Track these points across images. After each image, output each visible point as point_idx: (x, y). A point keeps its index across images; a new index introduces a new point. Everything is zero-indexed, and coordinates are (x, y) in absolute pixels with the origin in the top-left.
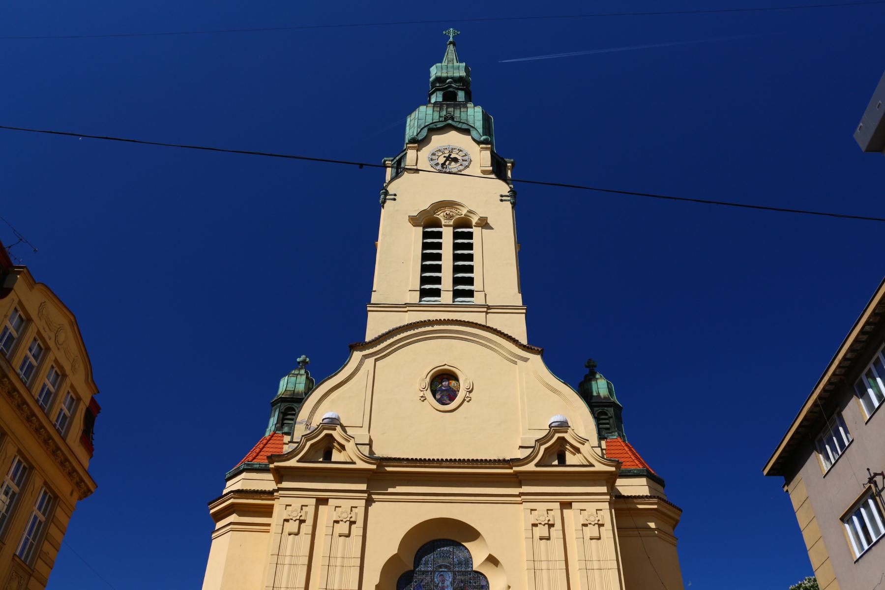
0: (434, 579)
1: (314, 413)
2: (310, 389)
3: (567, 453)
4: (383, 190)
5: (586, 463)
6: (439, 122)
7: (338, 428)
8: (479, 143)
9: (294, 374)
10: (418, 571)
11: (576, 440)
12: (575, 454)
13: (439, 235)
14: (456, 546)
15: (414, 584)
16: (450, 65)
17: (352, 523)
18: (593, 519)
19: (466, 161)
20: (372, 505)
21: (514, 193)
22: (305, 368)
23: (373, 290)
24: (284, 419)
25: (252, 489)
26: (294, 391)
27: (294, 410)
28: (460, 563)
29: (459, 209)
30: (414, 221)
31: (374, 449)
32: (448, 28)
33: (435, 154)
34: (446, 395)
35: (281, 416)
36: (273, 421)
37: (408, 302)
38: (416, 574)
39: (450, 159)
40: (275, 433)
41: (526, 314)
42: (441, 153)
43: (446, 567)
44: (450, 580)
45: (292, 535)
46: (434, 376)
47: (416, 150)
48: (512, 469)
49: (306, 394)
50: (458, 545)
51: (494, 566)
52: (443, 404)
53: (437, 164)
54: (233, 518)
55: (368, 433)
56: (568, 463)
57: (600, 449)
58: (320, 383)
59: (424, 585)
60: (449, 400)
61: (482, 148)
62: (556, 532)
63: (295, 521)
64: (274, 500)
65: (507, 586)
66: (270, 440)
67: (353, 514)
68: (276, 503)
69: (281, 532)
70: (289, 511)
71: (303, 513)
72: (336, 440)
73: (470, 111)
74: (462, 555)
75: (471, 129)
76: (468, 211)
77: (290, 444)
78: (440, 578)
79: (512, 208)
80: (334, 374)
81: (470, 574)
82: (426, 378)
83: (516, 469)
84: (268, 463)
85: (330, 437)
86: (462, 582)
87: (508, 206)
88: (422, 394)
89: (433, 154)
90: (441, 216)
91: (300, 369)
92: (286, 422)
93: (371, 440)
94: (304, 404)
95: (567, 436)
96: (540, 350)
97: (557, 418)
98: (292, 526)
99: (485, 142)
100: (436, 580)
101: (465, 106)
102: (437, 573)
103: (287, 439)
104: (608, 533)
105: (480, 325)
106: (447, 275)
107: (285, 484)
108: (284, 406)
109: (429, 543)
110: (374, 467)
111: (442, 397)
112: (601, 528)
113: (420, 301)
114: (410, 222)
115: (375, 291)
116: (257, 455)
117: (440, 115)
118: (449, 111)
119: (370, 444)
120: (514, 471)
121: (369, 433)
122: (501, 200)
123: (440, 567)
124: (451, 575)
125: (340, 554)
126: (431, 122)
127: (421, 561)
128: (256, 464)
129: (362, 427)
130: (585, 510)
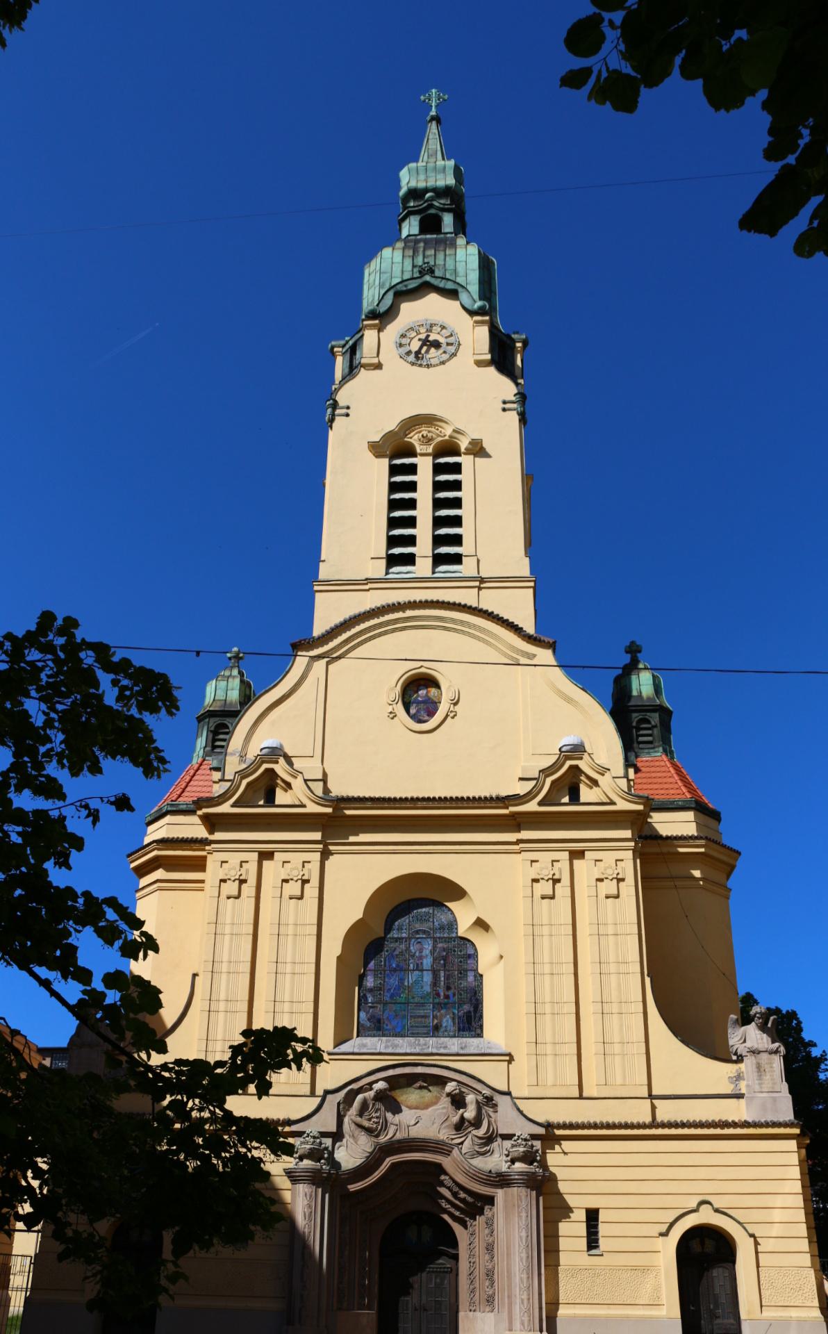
0: (409, 947)
1: (249, 741)
3: (582, 786)
4: (329, 400)
5: (605, 800)
6: (413, 278)
7: (282, 760)
8: (471, 313)
10: (390, 938)
11: (593, 769)
12: (591, 788)
13: (412, 469)
15: (384, 954)
16: (431, 165)
17: (305, 882)
19: (452, 344)
20: (329, 858)
21: (522, 397)
23: (322, 559)
28: (442, 928)
29: (441, 427)
30: (377, 449)
31: (330, 785)
32: (427, 90)
33: (406, 335)
34: (424, 709)
37: (370, 576)
38: (388, 941)
39: (428, 343)
41: (534, 588)
42: (415, 334)
43: (424, 932)
44: (430, 948)
45: (232, 899)
46: (408, 682)
47: (376, 331)
48: (508, 808)
50: (440, 905)
51: (484, 931)
52: (420, 721)
53: (409, 353)
55: (321, 765)
56: (582, 799)
57: (625, 780)
59: (397, 955)
60: (428, 715)
61: (476, 322)
62: (563, 890)
63: (234, 881)
65: (498, 956)
67: (305, 871)
70: (225, 869)
71: (243, 871)
72: (280, 777)
73: (460, 253)
74: (443, 918)
75: (460, 290)
76: (454, 431)
77: (221, 783)
78: (418, 946)
79: (520, 421)
81: (454, 941)
82: (396, 686)
83: (513, 809)
84: (195, 809)
85: (271, 773)
86: (444, 950)
87: (514, 417)
88: (390, 709)
89: (403, 336)
90: (415, 440)
93: (325, 774)
95: (582, 765)
96: (551, 642)
98: (232, 888)
99: (480, 312)
100: (412, 948)
101: (453, 245)
102: (413, 940)
103: (217, 776)
104: (629, 890)
105: (470, 607)
106: (424, 531)
107: (219, 836)
109: (402, 903)
110: (329, 810)
111: (418, 711)
112: (621, 884)
113: (387, 573)
114: (371, 451)
117: (413, 263)
118: (428, 256)
119: (324, 780)
121: (322, 764)
122: (504, 410)
124: (430, 942)
125: (291, 921)
126: (399, 280)
127: (394, 927)
130: (601, 861)
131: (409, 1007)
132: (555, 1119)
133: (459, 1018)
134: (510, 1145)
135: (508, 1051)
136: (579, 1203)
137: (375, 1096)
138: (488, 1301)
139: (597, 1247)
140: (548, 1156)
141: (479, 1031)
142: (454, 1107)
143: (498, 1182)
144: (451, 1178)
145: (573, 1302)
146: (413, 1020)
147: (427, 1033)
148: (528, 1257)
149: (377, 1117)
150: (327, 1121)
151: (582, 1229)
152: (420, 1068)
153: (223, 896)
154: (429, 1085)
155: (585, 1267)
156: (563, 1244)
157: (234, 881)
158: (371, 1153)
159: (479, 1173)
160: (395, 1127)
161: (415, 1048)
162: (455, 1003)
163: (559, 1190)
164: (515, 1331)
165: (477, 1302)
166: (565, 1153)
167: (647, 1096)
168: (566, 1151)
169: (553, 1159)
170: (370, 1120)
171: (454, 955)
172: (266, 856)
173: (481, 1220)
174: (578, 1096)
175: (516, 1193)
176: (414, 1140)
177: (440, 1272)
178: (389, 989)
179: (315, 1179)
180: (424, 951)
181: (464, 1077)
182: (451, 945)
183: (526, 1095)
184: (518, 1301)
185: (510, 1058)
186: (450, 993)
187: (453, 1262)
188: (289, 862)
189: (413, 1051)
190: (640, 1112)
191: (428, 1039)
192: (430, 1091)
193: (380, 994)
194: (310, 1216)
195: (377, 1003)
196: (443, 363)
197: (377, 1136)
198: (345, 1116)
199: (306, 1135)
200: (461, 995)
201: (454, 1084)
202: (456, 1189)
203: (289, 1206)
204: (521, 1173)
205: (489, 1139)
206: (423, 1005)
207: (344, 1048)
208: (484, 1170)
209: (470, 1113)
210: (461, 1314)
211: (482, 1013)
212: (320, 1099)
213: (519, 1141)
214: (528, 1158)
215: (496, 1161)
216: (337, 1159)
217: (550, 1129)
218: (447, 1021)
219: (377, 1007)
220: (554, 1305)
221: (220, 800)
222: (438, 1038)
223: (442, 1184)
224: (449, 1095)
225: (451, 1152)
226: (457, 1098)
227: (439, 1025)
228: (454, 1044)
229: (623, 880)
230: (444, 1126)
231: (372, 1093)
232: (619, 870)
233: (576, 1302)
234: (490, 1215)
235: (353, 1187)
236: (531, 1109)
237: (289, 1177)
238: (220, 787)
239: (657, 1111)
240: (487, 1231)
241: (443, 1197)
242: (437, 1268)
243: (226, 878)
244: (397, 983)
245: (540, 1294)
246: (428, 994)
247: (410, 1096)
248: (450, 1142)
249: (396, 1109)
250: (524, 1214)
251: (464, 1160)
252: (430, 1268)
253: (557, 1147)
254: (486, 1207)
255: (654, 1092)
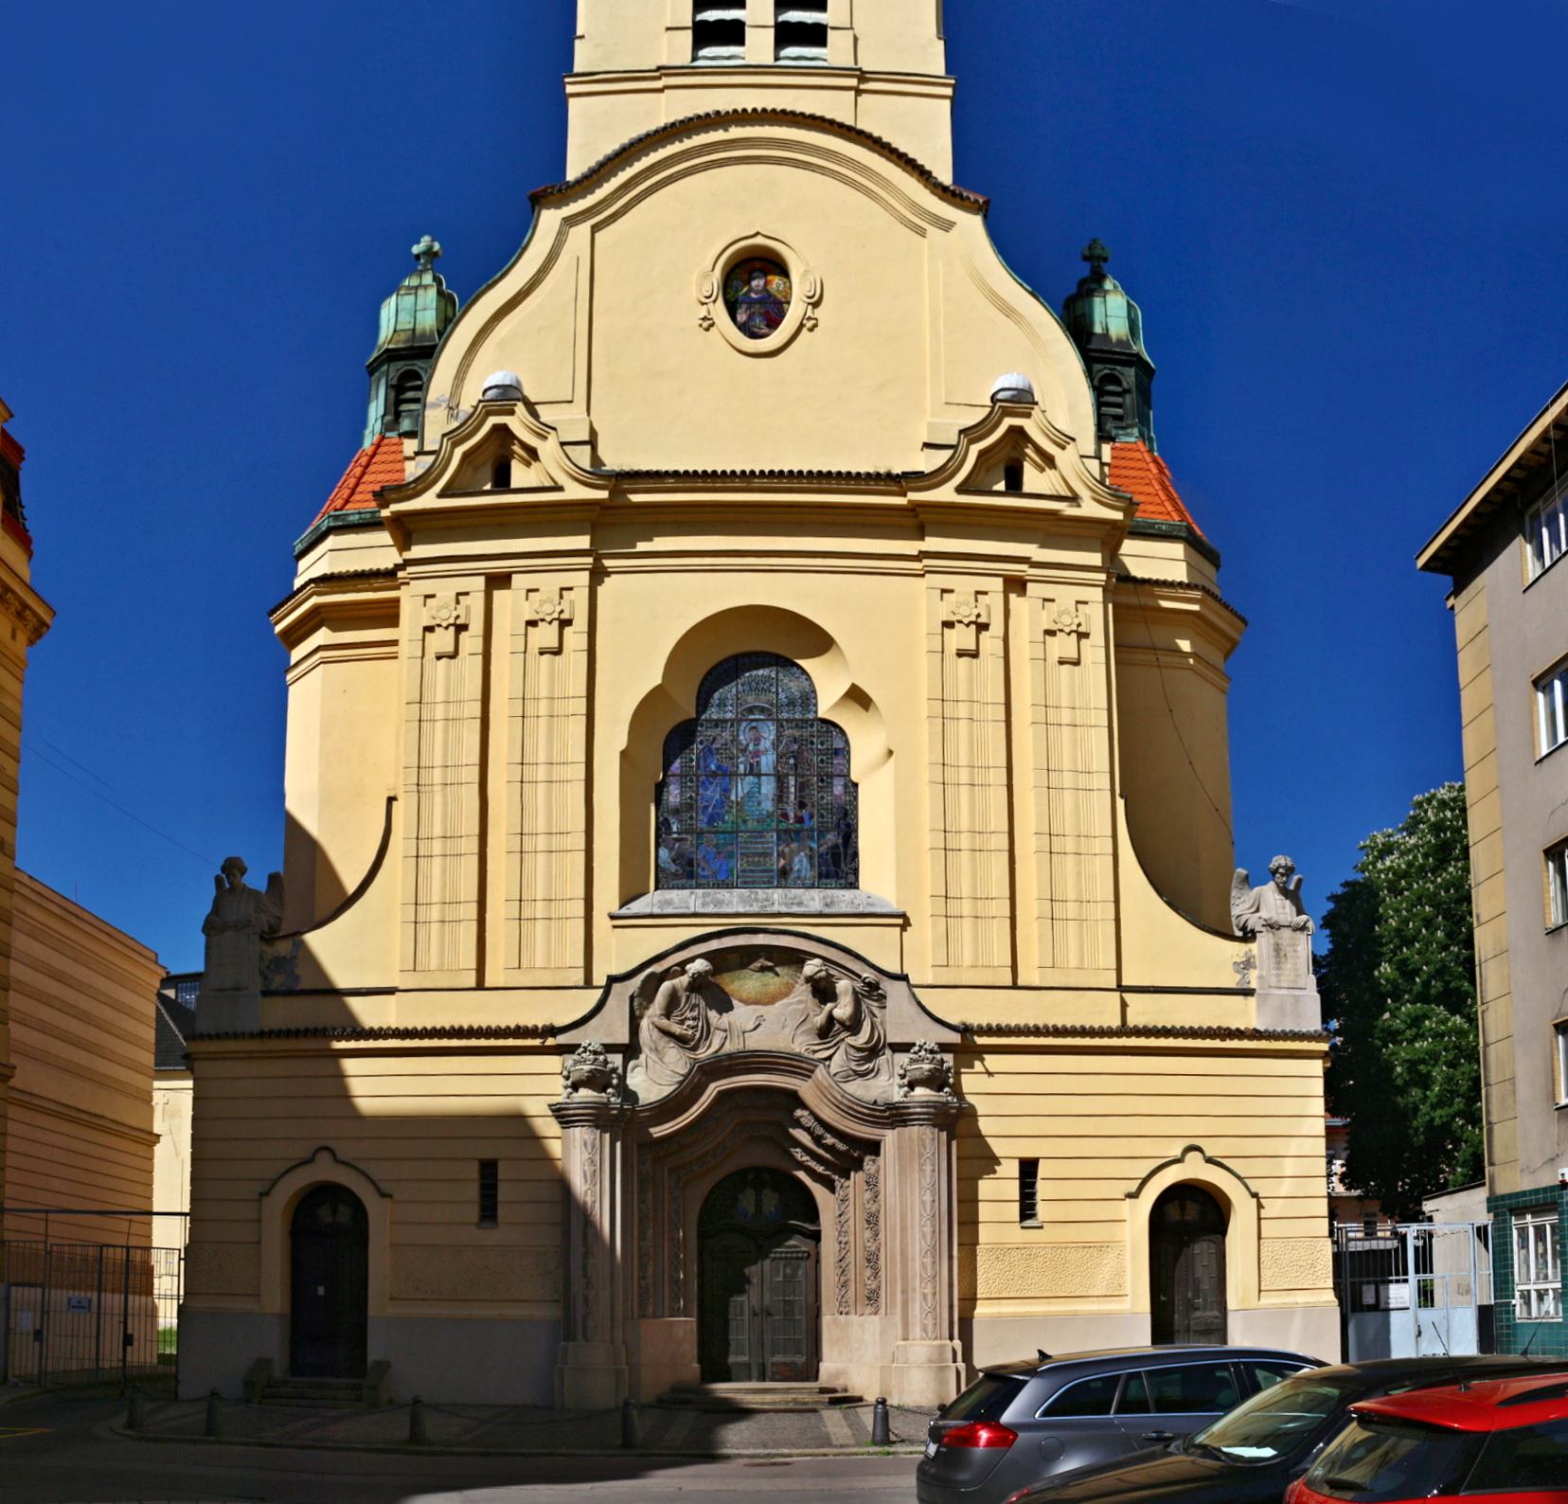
1: (463, 380)
2: (448, 322)
7: (520, 408)
9: (409, 288)
14: (784, 666)
17: (565, 623)
18: (1068, 621)
20: (603, 582)
22: (432, 269)
23: (579, 33)
24: (398, 402)
25: (352, 570)
26: (414, 330)
27: (420, 378)
31: (602, 452)
35: (392, 395)
36: (376, 409)
40: (383, 438)
45: (444, 659)
49: (440, 334)
54: (323, 636)
58: (470, 299)
64: (398, 588)
66: (374, 454)
67: (565, 605)
68: (403, 594)
69: (420, 655)
71: (461, 610)
77: (418, 458)
80: (499, 274)
84: (377, 509)
85: (503, 432)
91: (421, 274)
92: (404, 407)
93: (593, 433)
94: (439, 357)
97: (1011, 380)
98: (442, 640)
103: (410, 446)
107: (418, 551)
108: (395, 369)
112: (1084, 642)
115: (582, 37)
116: (352, 494)
119: (592, 442)
120: (909, 501)
121: (589, 414)
125: (543, 693)
128: (353, 514)
129: (571, 402)
130: (1053, 600)
131: (739, 839)
132: (976, 1019)
133: (821, 856)
134: (907, 1061)
135: (900, 910)
136: (1008, 1152)
137: (690, 983)
138: (869, 1299)
139: (1033, 1216)
140: (964, 1078)
141: (851, 878)
142: (817, 1001)
143: (887, 1118)
144: (813, 1114)
145: (997, 1296)
146: (745, 860)
147: (769, 882)
148: (934, 1232)
149: (694, 1019)
150: (613, 1026)
151: (1013, 1190)
152: (761, 936)
153: (430, 655)
154: (776, 966)
155: (1016, 1246)
156: (984, 1211)
157: (447, 628)
158: (686, 1076)
159: (857, 1105)
160: (723, 1034)
161: (751, 906)
162: (812, 830)
163: (980, 1131)
164: (914, 1340)
165: (852, 1301)
166: (990, 1074)
167: (1114, 986)
168: (991, 1070)
169: (970, 1082)
170: (682, 1022)
171: (812, 749)
172: (498, 581)
173: (857, 1177)
174: (1010, 984)
175: (916, 1137)
176: (755, 1054)
177: (792, 1258)
178: (706, 807)
179: (600, 1118)
180: (762, 742)
181: (833, 950)
183: (930, 982)
184: (918, 1297)
185: (904, 922)
186: (804, 813)
187: (812, 1243)
188: (537, 590)
189: (748, 909)
190: (1104, 1012)
191: (770, 891)
192: (777, 975)
193: (691, 818)
194: (593, 1178)
195: (687, 832)
197: (694, 1049)
198: (641, 1017)
199: (581, 1050)
200: (822, 816)
201: (817, 961)
202: (819, 1131)
203: (559, 1163)
204: (926, 1104)
205: (872, 1051)
206: (760, 834)
207: (636, 907)
208: (865, 1099)
209: (843, 1010)
210: (826, 1320)
211: (856, 848)
212: (602, 990)
213: (923, 1053)
214: (936, 1080)
215: (886, 1085)
216: (631, 1087)
217: (968, 1035)
218: (801, 861)
219: (686, 839)
220: (969, 1300)
221: (419, 487)
222: (786, 890)
223: (797, 1124)
224: (809, 980)
225: (812, 1072)
226: (823, 984)
227: (788, 867)
228: (813, 899)
229: (1086, 635)
230: (803, 1028)
231: (685, 980)
232: (1082, 619)
233: (1001, 1296)
234: (872, 1171)
235: (658, 1131)
236: (941, 1004)
237: (557, 1117)
238: (417, 466)
239: (1129, 1010)
240: (868, 1195)
241: (798, 1144)
242: (787, 1252)
243: (433, 623)
244: (718, 796)
245: (951, 1286)
246: (769, 815)
247: (746, 983)
248: (811, 1056)
249: (724, 1005)
250: (928, 1168)
251: (833, 1084)
252: (776, 1253)
253: (977, 1064)
254: (867, 1158)
255: (1125, 983)
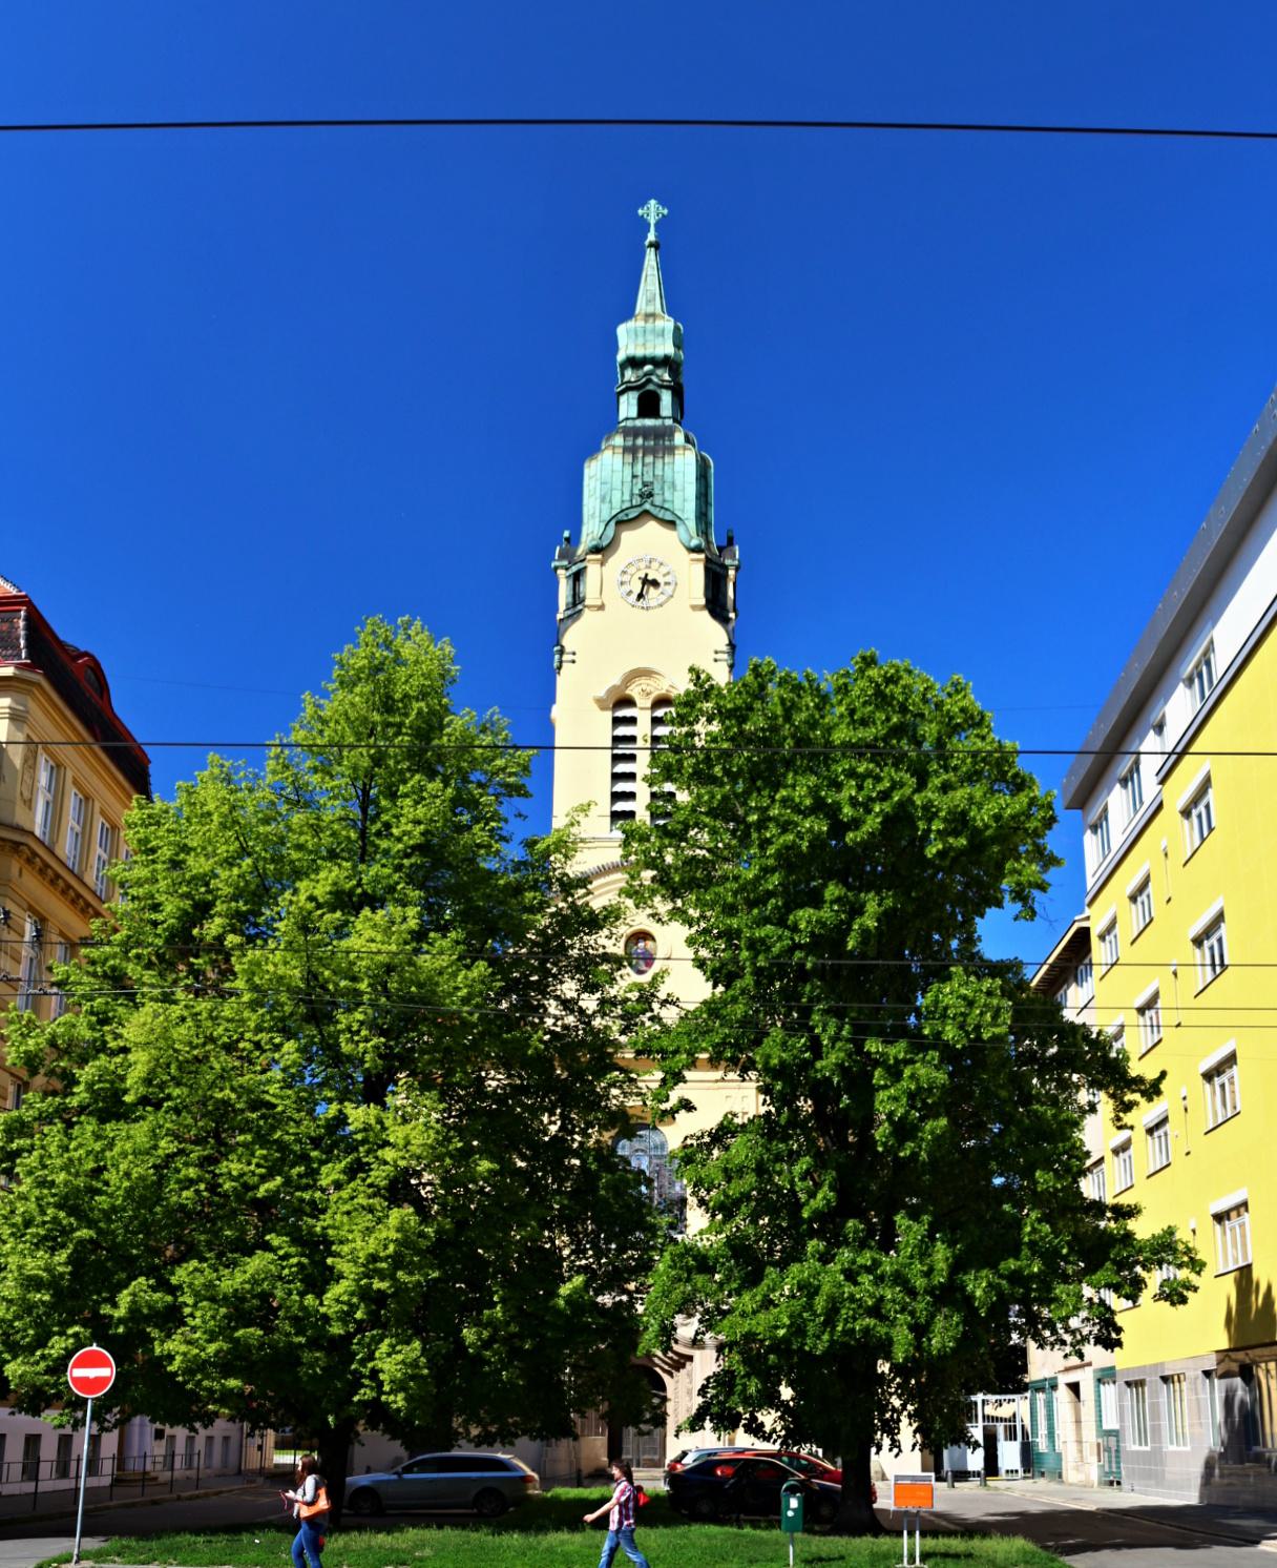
6: (632, 507)
28: (656, 1147)
61: (693, 560)
75: (678, 522)
99: (696, 550)
123: (637, 1151)
124: (647, 1158)
182: (663, 1161)
196: (661, 605)
